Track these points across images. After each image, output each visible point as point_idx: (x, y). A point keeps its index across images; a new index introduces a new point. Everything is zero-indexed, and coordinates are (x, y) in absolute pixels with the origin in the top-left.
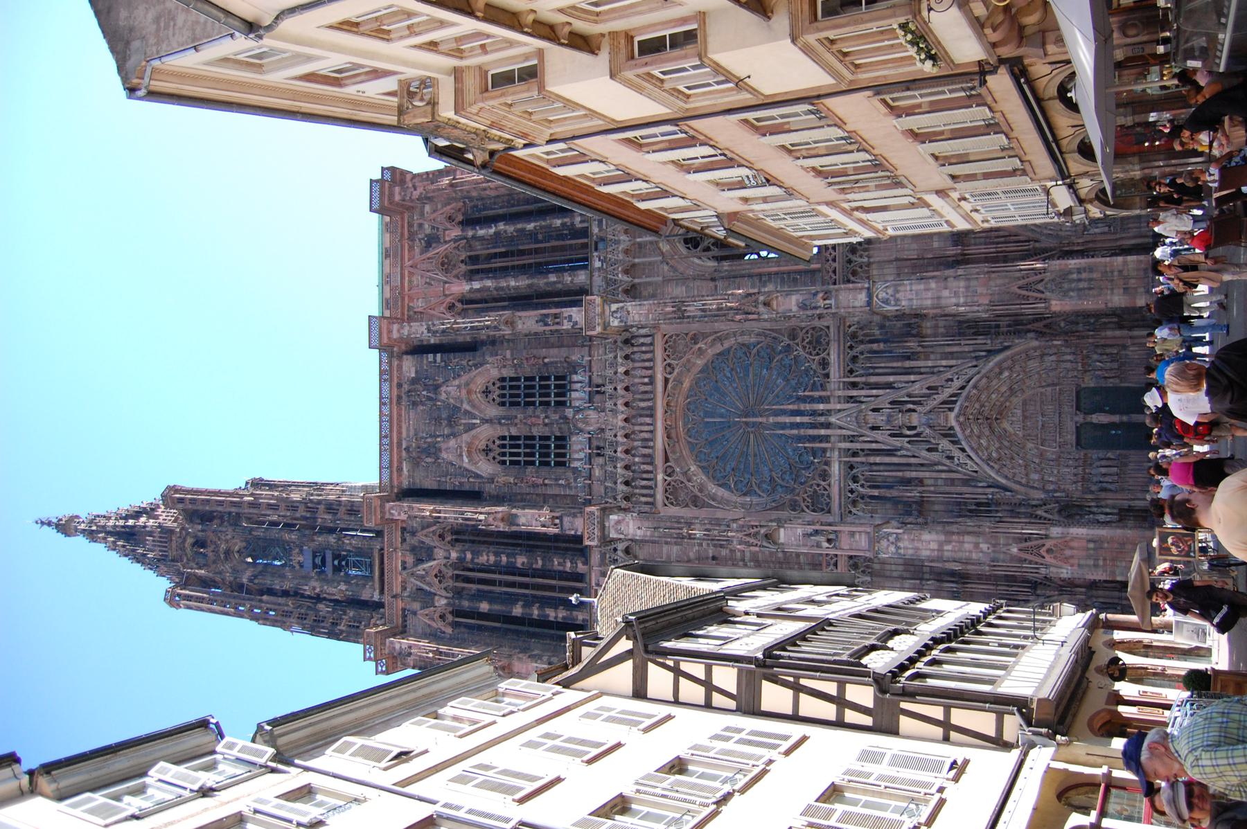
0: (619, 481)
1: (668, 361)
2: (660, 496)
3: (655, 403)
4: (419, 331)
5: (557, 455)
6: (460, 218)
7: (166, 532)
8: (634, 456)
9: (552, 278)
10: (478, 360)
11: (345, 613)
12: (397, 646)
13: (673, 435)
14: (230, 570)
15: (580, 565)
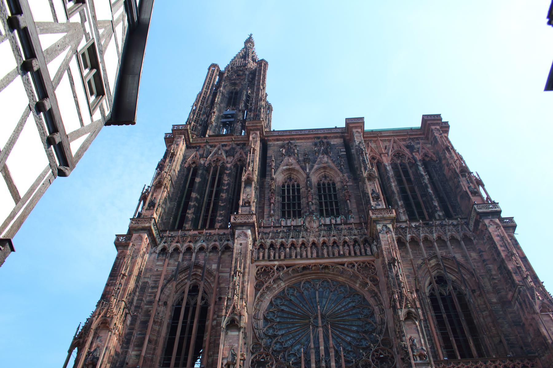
0: (273, 241)
1: (356, 265)
2: (263, 263)
3: (326, 258)
4: (358, 139)
5: (289, 212)
6: (427, 159)
7: (246, 65)
8: (290, 248)
9: (400, 203)
10: (345, 170)
11: (200, 125)
12: (179, 140)
13: (305, 272)
14: (225, 84)
15: (220, 224)
